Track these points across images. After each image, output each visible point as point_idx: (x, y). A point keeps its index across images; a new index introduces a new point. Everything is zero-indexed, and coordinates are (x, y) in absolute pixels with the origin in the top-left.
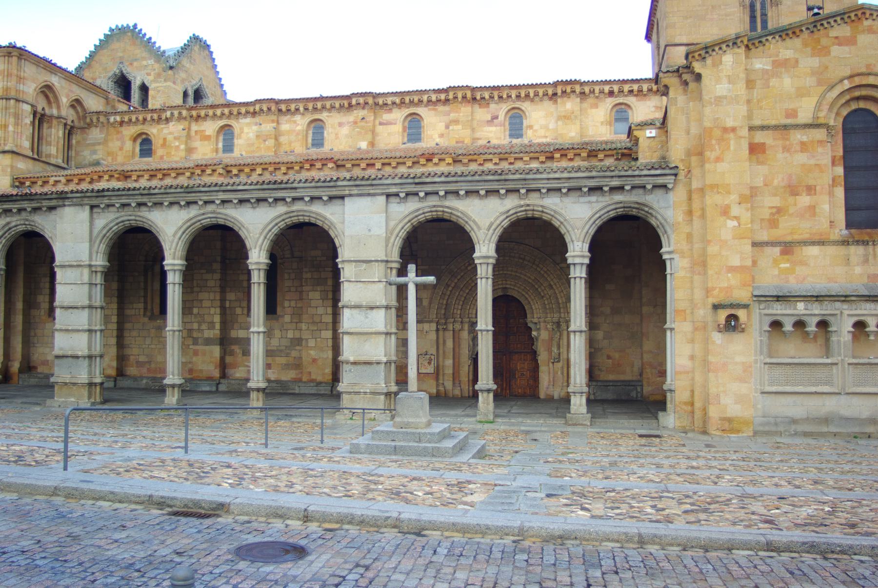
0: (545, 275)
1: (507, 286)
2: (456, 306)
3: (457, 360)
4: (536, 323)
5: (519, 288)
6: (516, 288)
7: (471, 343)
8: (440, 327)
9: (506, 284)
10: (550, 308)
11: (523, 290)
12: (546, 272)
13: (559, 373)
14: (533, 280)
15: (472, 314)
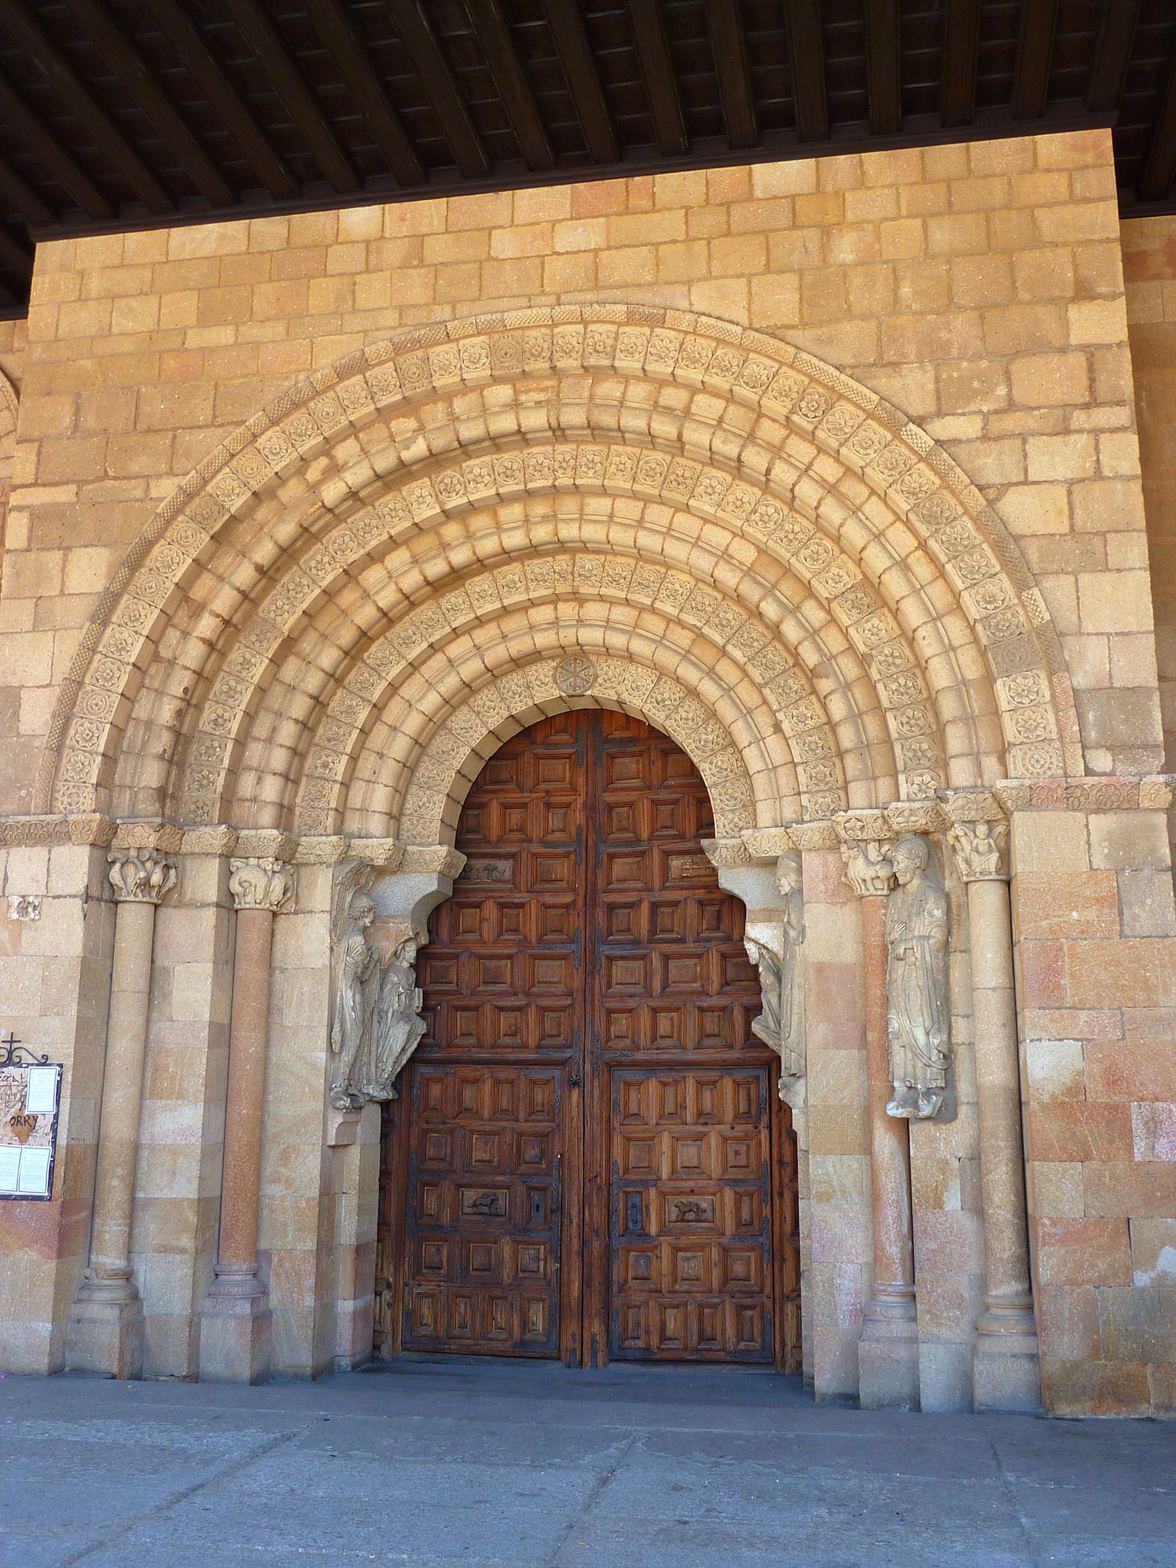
0: (832, 512)
1: (590, 636)
2: (254, 752)
3: (242, 1109)
4: (771, 863)
5: (661, 641)
6: (639, 647)
7: (348, 996)
8: (125, 877)
9: (580, 622)
10: (863, 748)
11: (686, 656)
12: (832, 489)
13: (953, 1200)
14: (749, 572)
15: (364, 810)
